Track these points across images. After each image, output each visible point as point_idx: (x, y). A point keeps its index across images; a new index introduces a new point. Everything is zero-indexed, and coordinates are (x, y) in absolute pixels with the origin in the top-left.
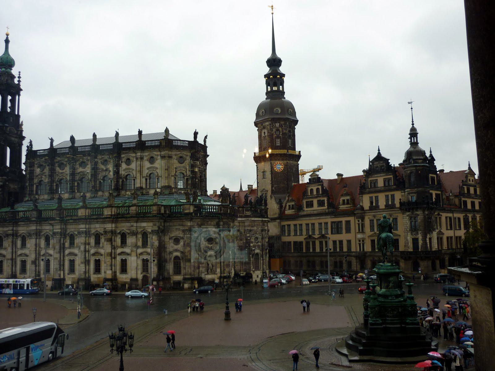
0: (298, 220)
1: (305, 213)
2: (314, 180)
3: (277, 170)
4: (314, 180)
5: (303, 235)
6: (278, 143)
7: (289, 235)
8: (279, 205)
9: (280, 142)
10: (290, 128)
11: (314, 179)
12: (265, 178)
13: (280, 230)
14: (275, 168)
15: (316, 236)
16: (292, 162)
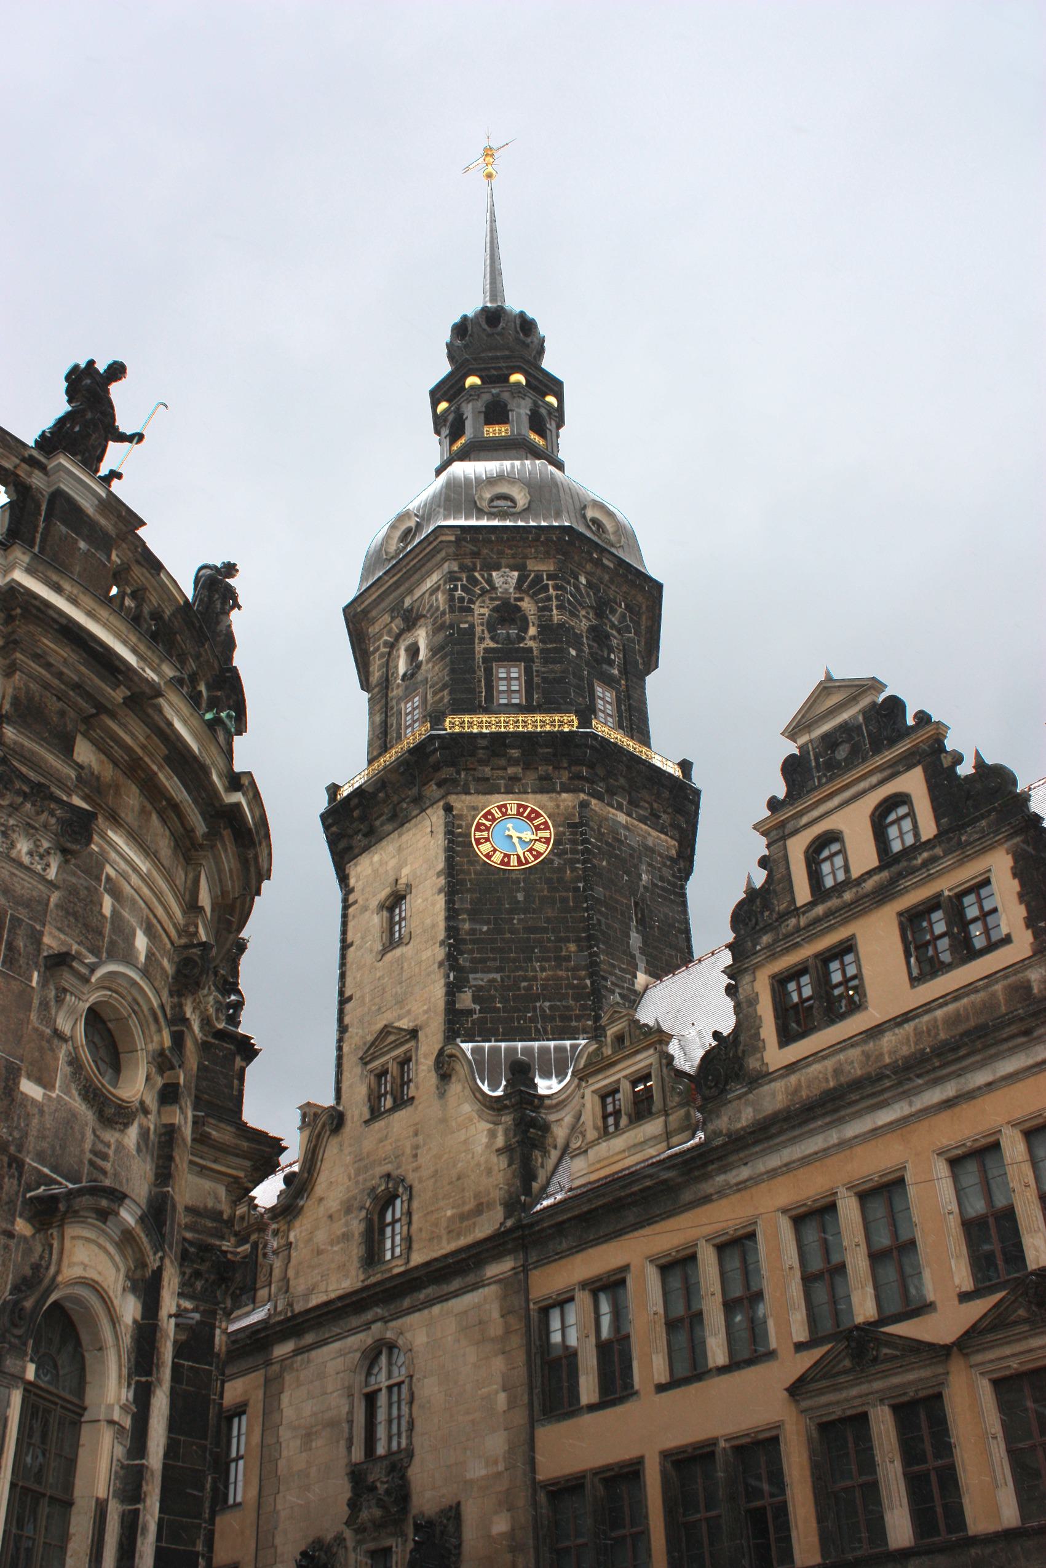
0: (707, 1199)
1: (774, 1097)
2: (842, 753)
3: (497, 858)
4: (842, 753)
5: (771, 1355)
6: (510, 692)
7: (617, 1386)
8: (507, 1119)
9: (529, 683)
10: (600, 613)
11: (830, 741)
12: (400, 942)
13: (520, 1358)
14: (485, 848)
15: (944, 1325)
16: (622, 818)
